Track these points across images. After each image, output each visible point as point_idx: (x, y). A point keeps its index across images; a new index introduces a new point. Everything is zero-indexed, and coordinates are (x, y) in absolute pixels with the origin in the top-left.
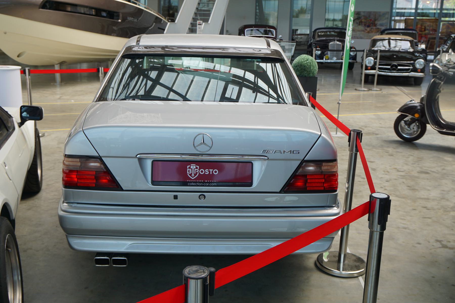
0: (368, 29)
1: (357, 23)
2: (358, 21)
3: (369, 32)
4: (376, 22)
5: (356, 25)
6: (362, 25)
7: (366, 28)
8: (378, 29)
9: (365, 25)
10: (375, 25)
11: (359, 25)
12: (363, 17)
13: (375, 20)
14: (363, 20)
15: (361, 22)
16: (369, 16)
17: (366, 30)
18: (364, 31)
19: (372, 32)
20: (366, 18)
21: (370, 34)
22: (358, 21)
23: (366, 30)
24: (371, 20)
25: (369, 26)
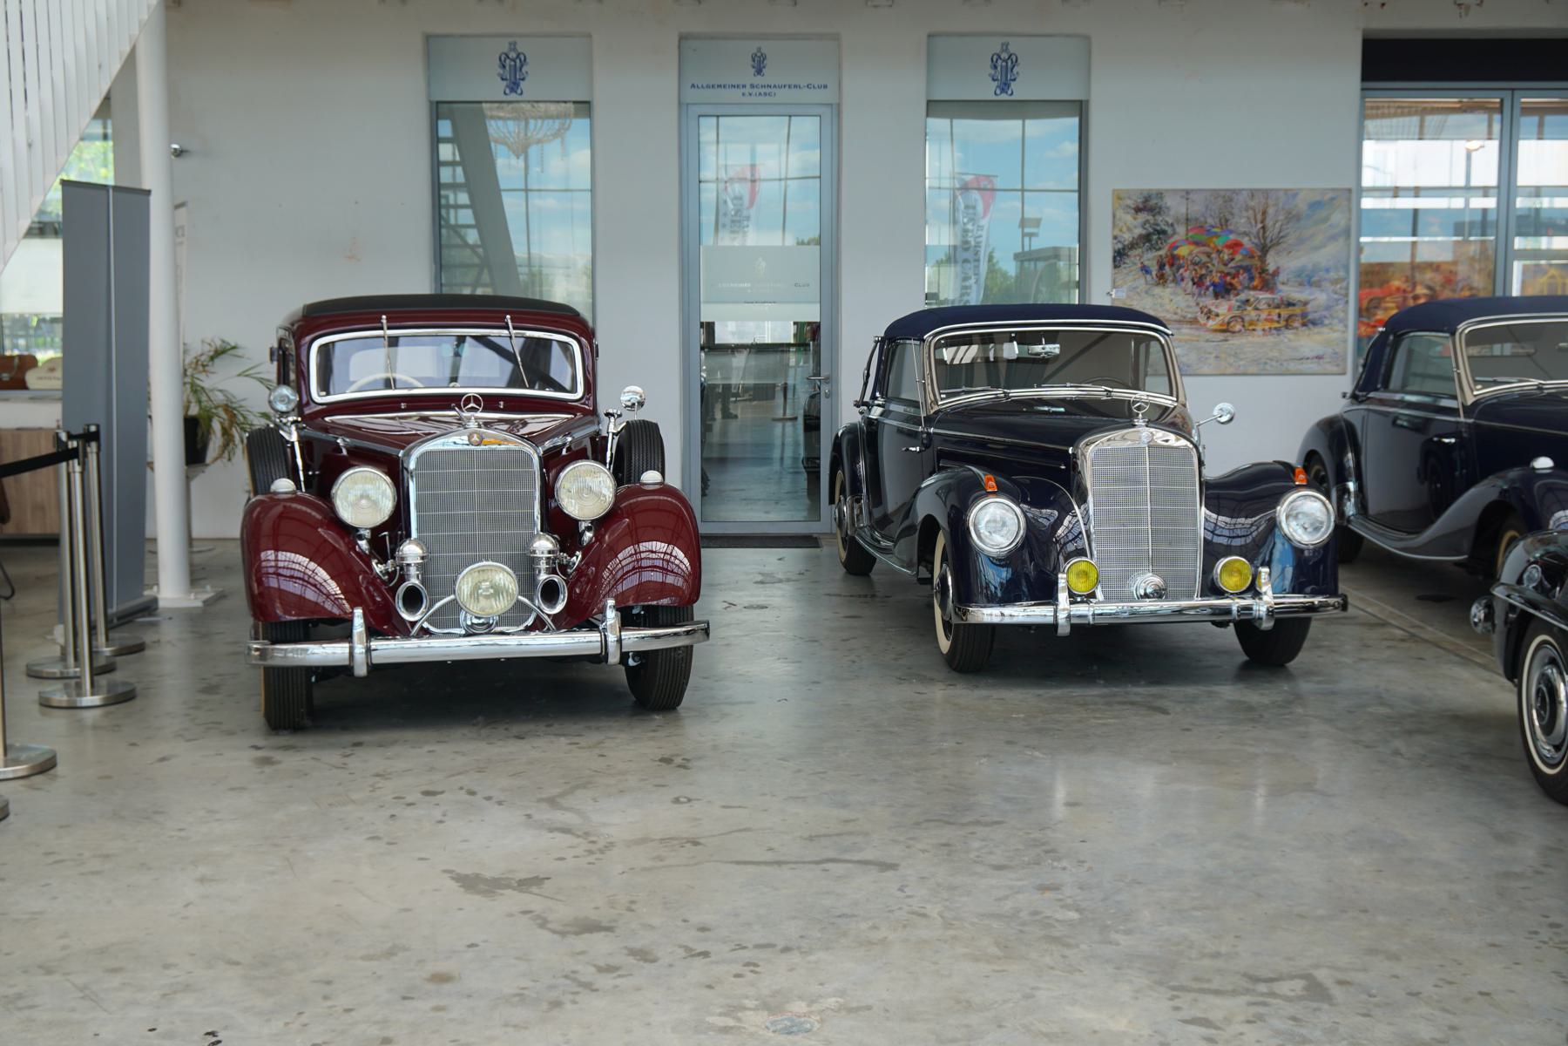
0: (1223, 308)
1: (1145, 270)
2: (1150, 258)
3: (1226, 329)
4: (1272, 262)
5: (1141, 283)
6: (1178, 280)
7: (1208, 301)
8: (1290, 304)
9: (1198, 282)
10: (1267, 282)
11: (1162, 279)
12: (1181, 230)
13: (1265, 250)
14: (1183, 251)
15: (1173, 260)
16: (1224, 223)
17: (1209, 314)
18: (1194, 321)
19: (1249, 327)
20: (1201, 232)
21: (1236, 341)
22: (1150, 258)
23: (1209, 314)
24: (1235, 246)
25: (1223, 290)
